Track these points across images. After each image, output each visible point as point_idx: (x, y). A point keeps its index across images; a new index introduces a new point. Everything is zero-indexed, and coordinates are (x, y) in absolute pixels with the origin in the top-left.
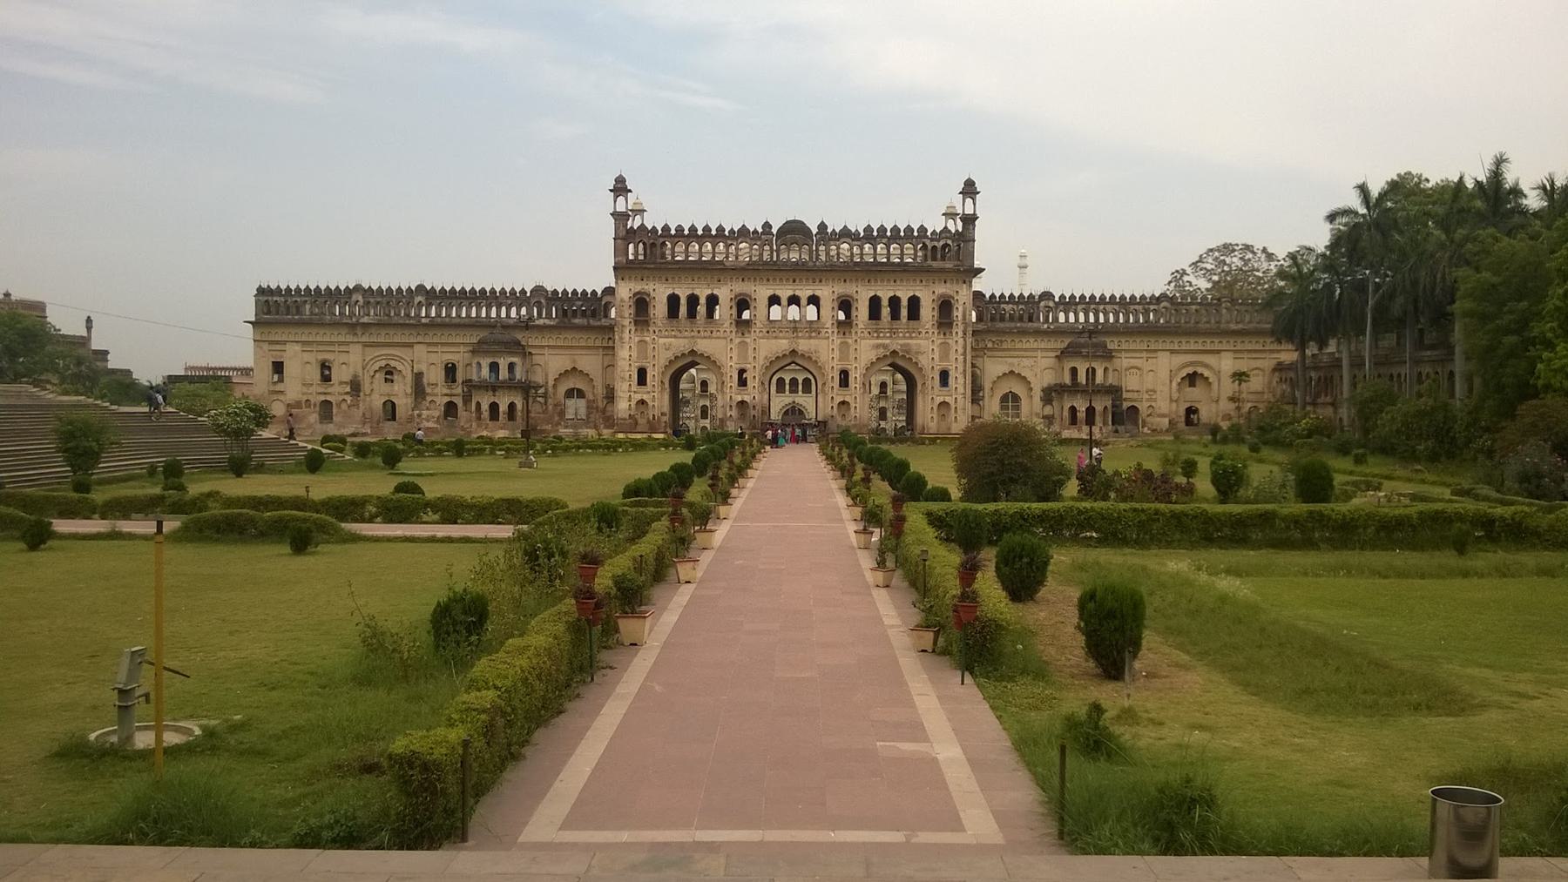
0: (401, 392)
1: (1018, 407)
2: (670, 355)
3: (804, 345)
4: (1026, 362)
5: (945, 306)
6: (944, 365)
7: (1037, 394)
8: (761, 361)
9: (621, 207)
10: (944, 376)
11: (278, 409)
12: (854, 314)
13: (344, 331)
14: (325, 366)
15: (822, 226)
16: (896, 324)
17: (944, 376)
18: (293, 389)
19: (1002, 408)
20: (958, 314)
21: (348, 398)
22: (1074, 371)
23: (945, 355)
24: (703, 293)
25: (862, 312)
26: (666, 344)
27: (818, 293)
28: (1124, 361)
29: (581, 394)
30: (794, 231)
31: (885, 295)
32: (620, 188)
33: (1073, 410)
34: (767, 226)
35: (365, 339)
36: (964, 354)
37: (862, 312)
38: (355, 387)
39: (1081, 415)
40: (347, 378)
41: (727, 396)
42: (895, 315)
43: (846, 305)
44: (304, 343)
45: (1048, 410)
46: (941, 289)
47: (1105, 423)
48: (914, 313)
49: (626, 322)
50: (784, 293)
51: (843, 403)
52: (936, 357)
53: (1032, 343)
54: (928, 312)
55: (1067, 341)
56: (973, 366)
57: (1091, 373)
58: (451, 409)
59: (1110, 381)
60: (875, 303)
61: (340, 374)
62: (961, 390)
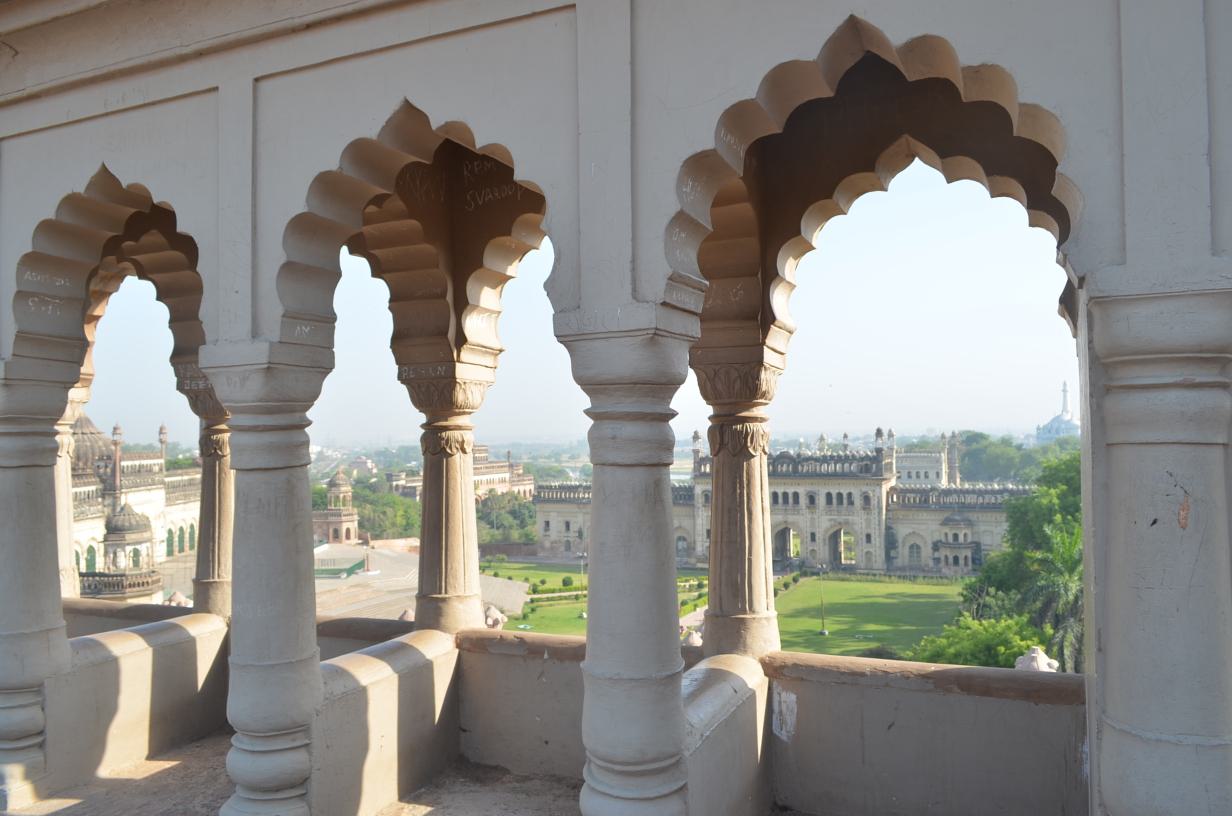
1: (918, 553)
3: (791, 518)
4: (923, 527)
5: (867, 499)
6: (869, 531)
7: (930, 546)
10: (868, 537)
11: (547, 544)
12: (817, 502)
13: (575, 506)
14: (568, 525)
17: (868, 537)
18: (554, 534)
19: (911, 552)
20: (874, 502)
21: (578, 540)
22: (946, 534)
23: (868, 525)
25: (821, 500)
27: (798, 491)
28: (982, 528)
29: (684, 539)
31: (834, 492)
33: (946, 557)
35: (584, 511)
36: (879, 525)
37: (821, 500)
38: (580, 534)
39: (951, 560)
40: (576, 529)
42: (840, 502)
43: (812, 499)
44: (558, 512)
45: (936, 555)
46: (864, 489)
47: (966, 564)
48: (851, 503)
49: (700, 505)
51: (813, 550)
52: (864, 526)
53: (924, 516)
55: (946, 515)
56: (888, 528)
57: (956, 536)
59: (969, 540)
60: (829, 496)
61: (574, 527)
62: (878, 544)
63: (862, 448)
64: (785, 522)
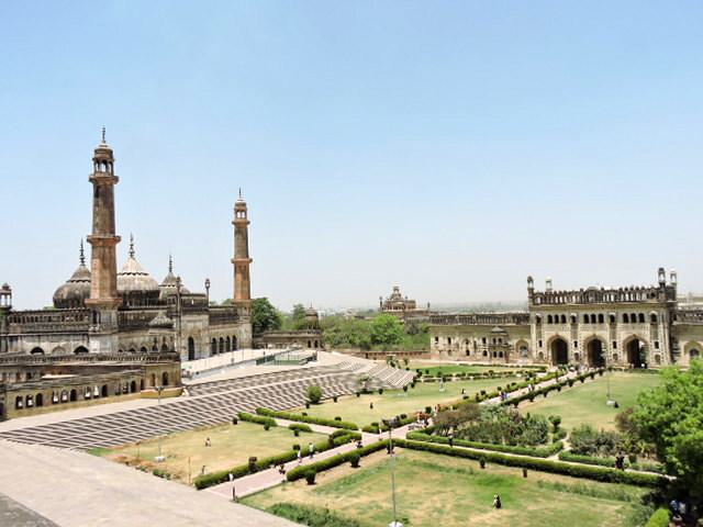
0: (471, 347)
2: (550, 336)
3: (598, 333)
8: (583, 339)
9: (531, 285)
15: (603, 289)
16: (635, 325)
24: (560, 314)
26: (549, 332)
30: (592, 292)
32: (530, 280)
34: (582, 290)
38: (458, 345)
41: (572, 351)
50: (590, 313)
54: (647, 318)
58: (485, 354)
63: (652, 282)
64: (594, 335)
